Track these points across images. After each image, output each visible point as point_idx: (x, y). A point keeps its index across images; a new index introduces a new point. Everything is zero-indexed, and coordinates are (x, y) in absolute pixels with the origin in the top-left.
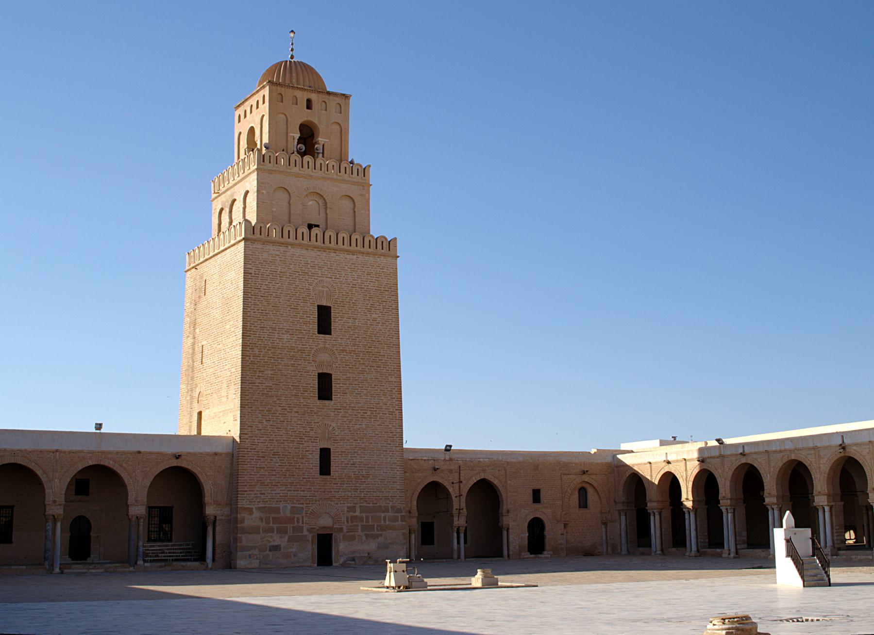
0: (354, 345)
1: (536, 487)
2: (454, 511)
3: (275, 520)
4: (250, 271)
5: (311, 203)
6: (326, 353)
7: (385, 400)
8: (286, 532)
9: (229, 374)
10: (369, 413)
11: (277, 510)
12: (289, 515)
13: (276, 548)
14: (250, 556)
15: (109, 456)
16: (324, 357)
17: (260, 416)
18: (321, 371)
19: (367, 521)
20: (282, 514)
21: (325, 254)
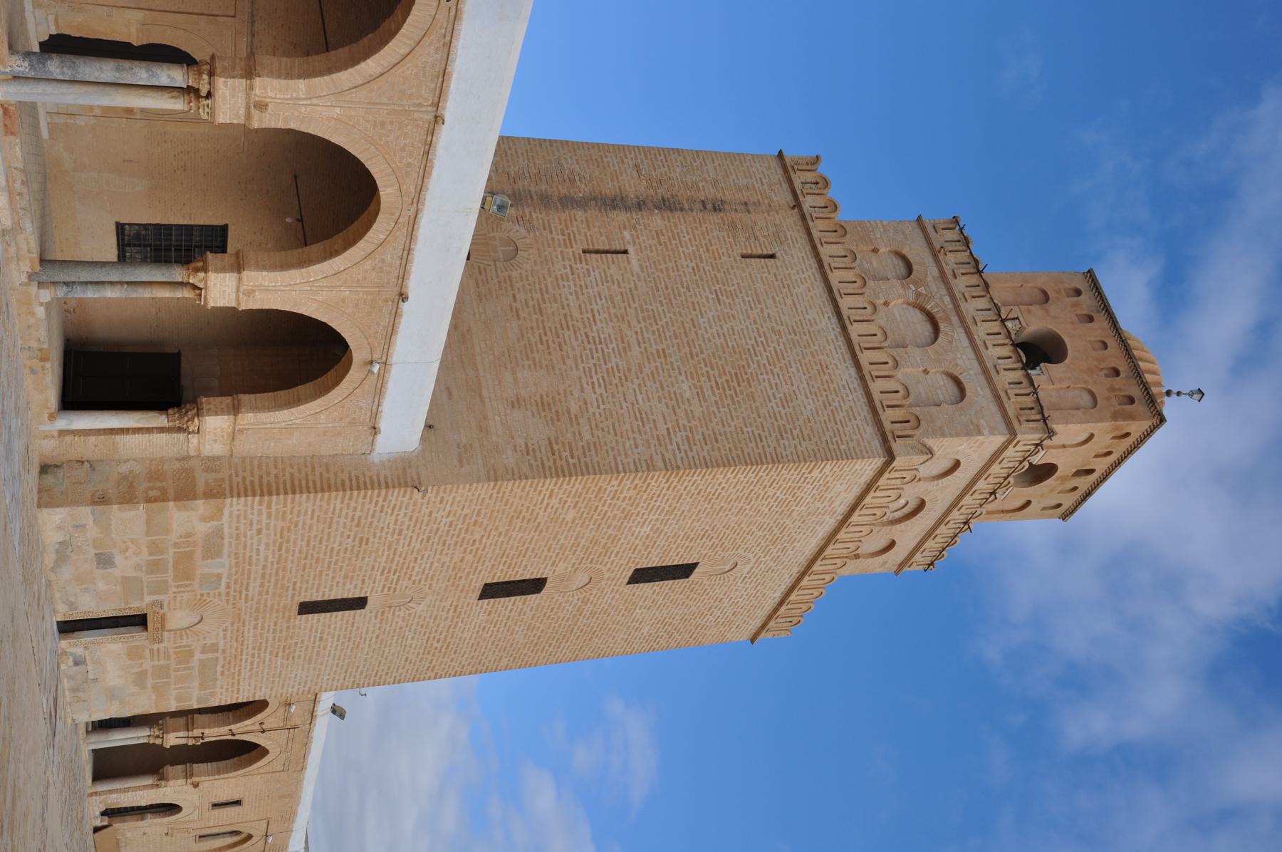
0: (593, 613)
1: (244, 803)
2: (197, 732)
4: (816, 473)
9: (574, 408)
10: (439, 645)
12: (199, 572)
13: (104, 561)
17: (466, 511)
19: (177, 670)
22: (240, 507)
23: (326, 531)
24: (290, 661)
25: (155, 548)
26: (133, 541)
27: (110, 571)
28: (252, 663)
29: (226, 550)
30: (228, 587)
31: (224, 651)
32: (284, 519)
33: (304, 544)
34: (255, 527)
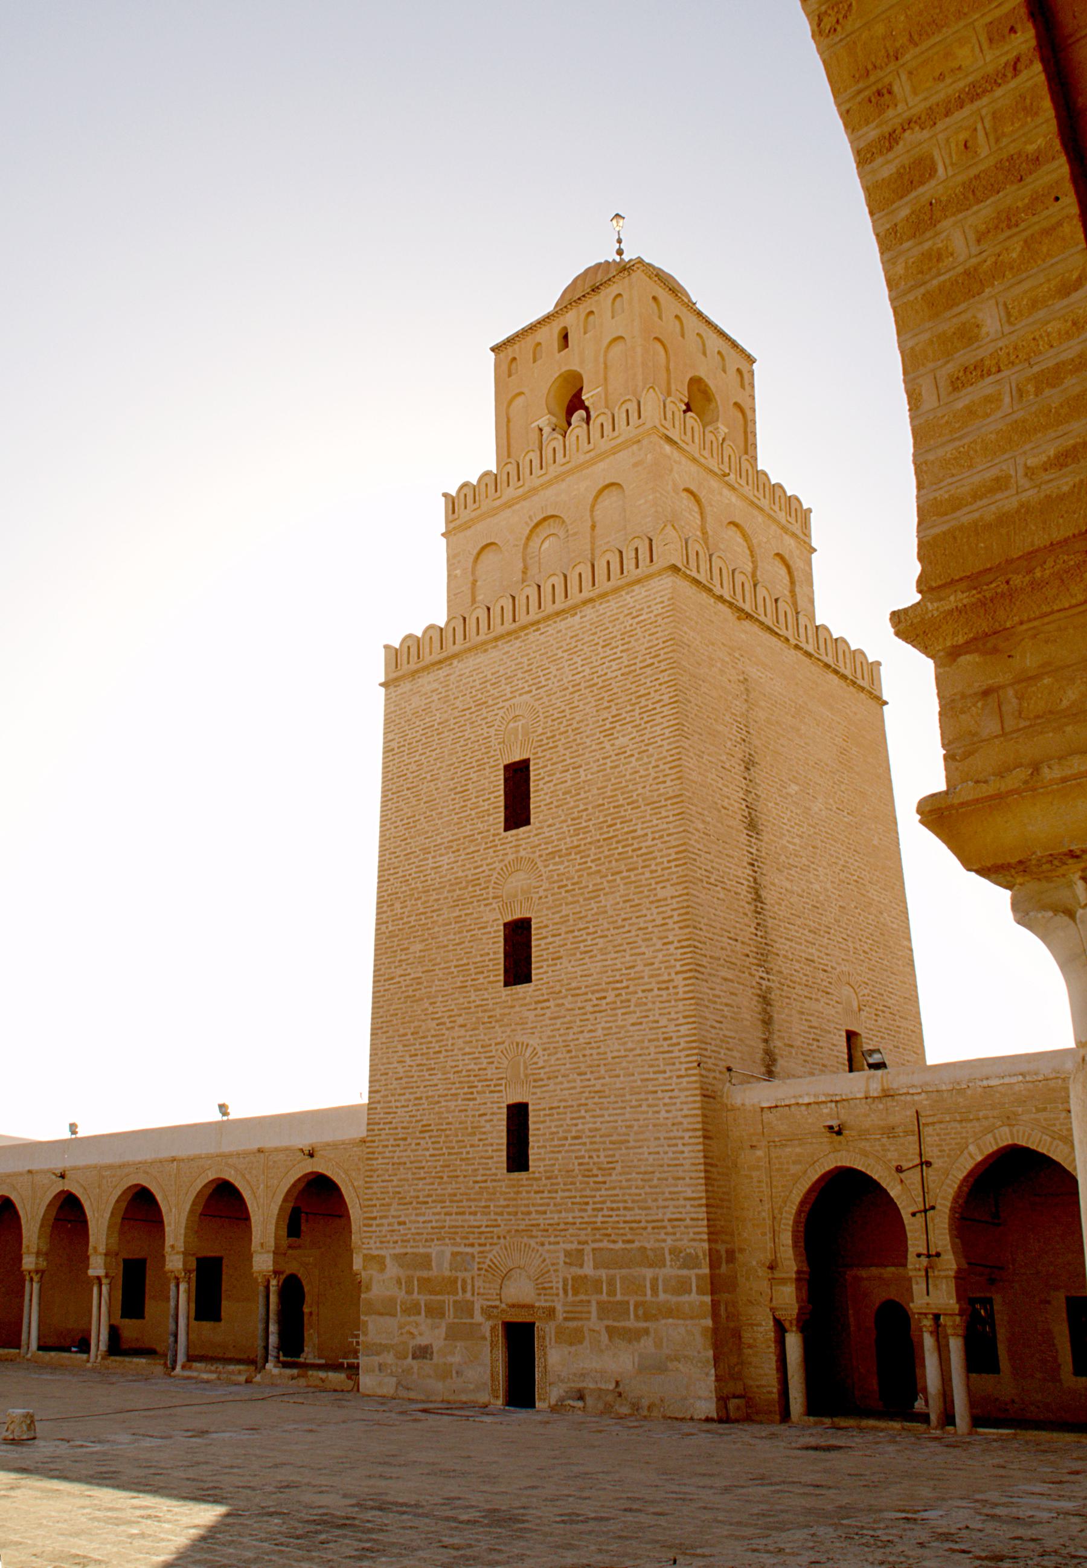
3: (424, 1283)
5: (546, 545)
6: (523, 873)
7: (649, 953)
8: (442, 1315)
10: (611, 996)
11: (425, 1261)
12: (447, 1273)
14: (380, 1365)
15: (230, 1161)
16: (518, 881)
17: (400, 1047)
18: (509, 919)
19: (612, 1292)
20: (434, 1273)
21: (518, 643)
22: (372, 1241)
23: (408, 1165)
24: (618, 1166)
25: (412, 1309)
26: (400, 1328)
27: (435, 1349)
28: (612, 1209)
29: (422, 1250)
30: (472, 1245)
31: (579, 1243)
32: (389, 1205)
33: (421, 1182)
34: (396, 1227)
